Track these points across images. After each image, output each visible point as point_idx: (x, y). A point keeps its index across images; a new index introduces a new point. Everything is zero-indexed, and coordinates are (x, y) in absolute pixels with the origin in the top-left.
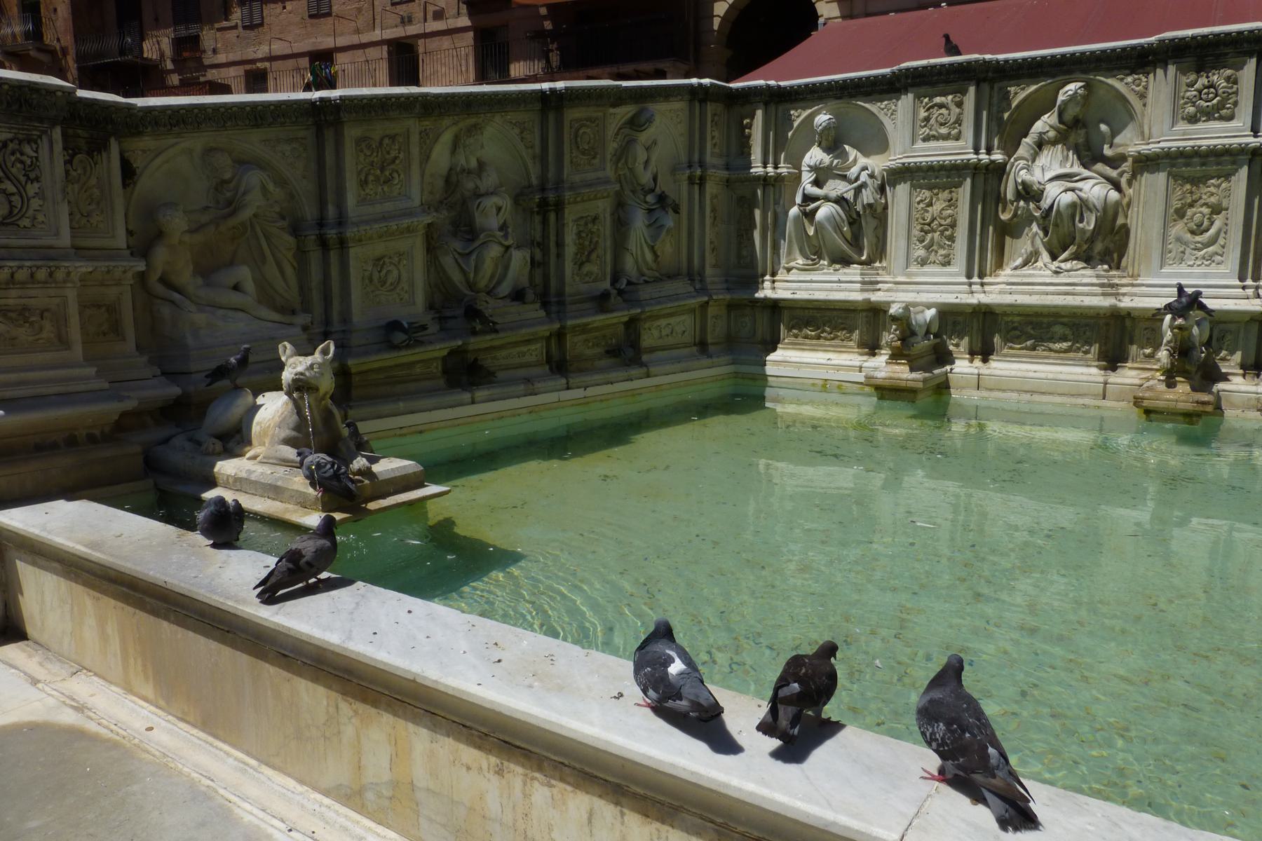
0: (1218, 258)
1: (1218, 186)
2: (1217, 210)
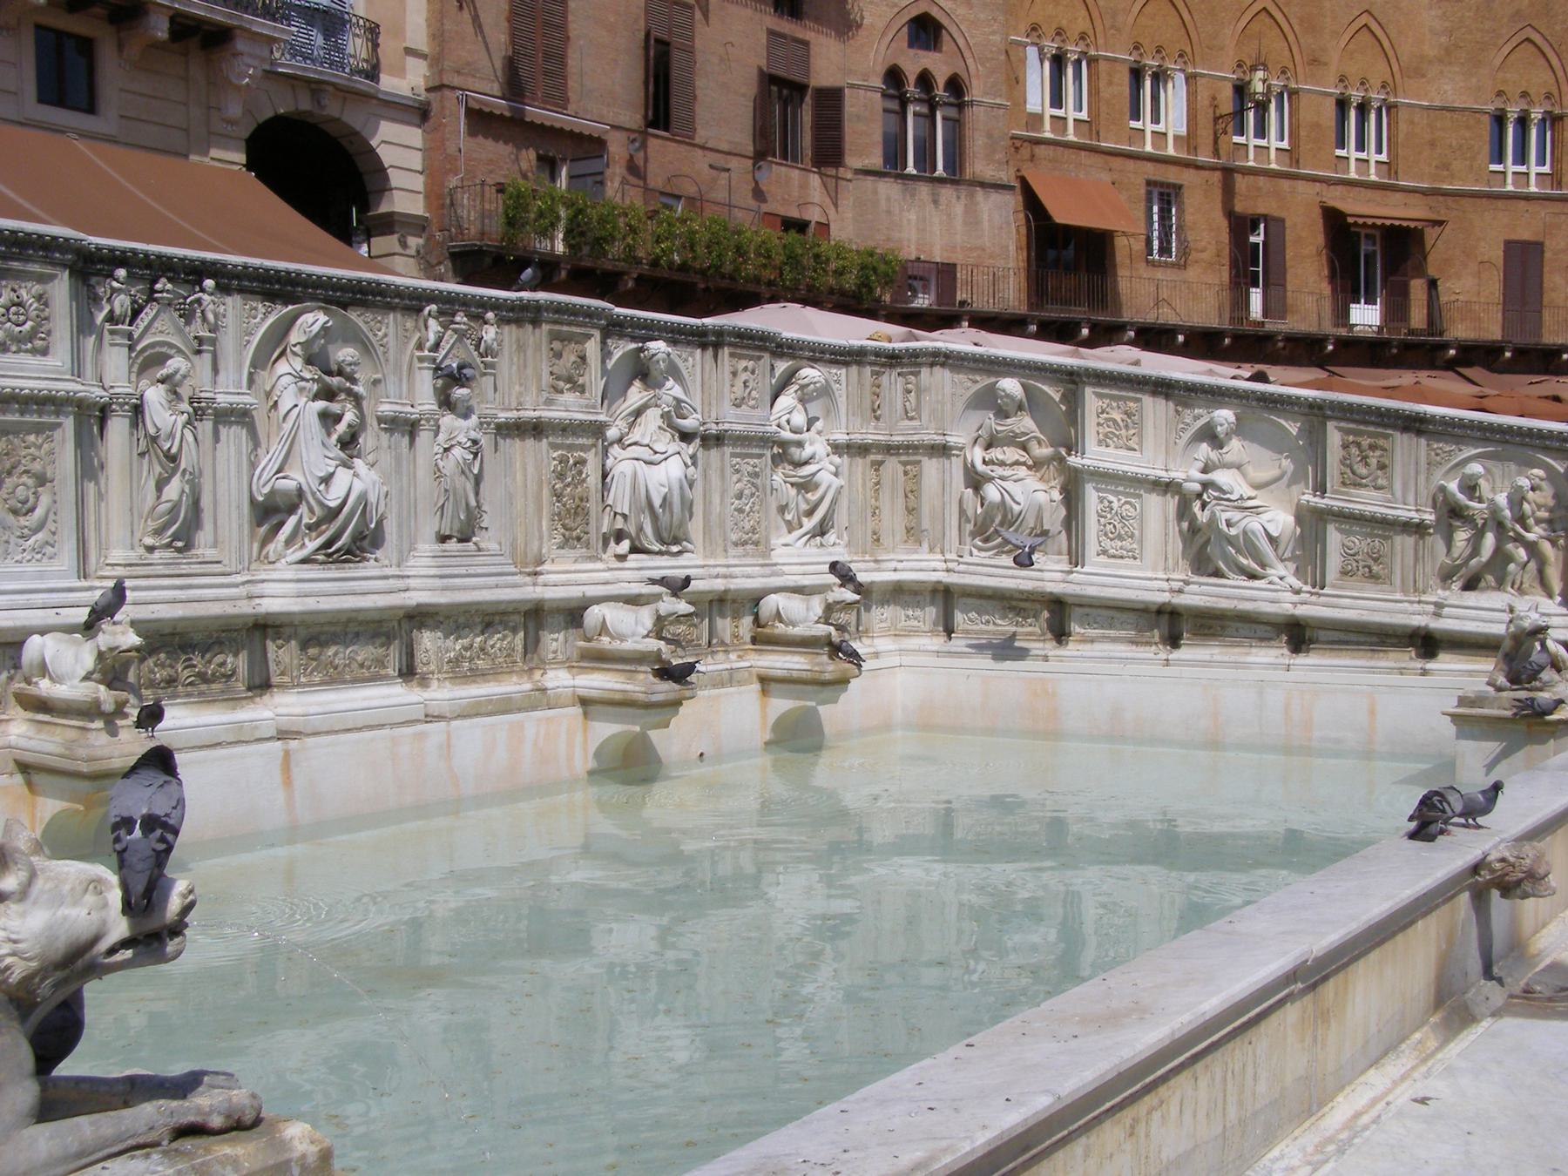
0: (49, 550)
1: (39, 447)
2: (42, 480)
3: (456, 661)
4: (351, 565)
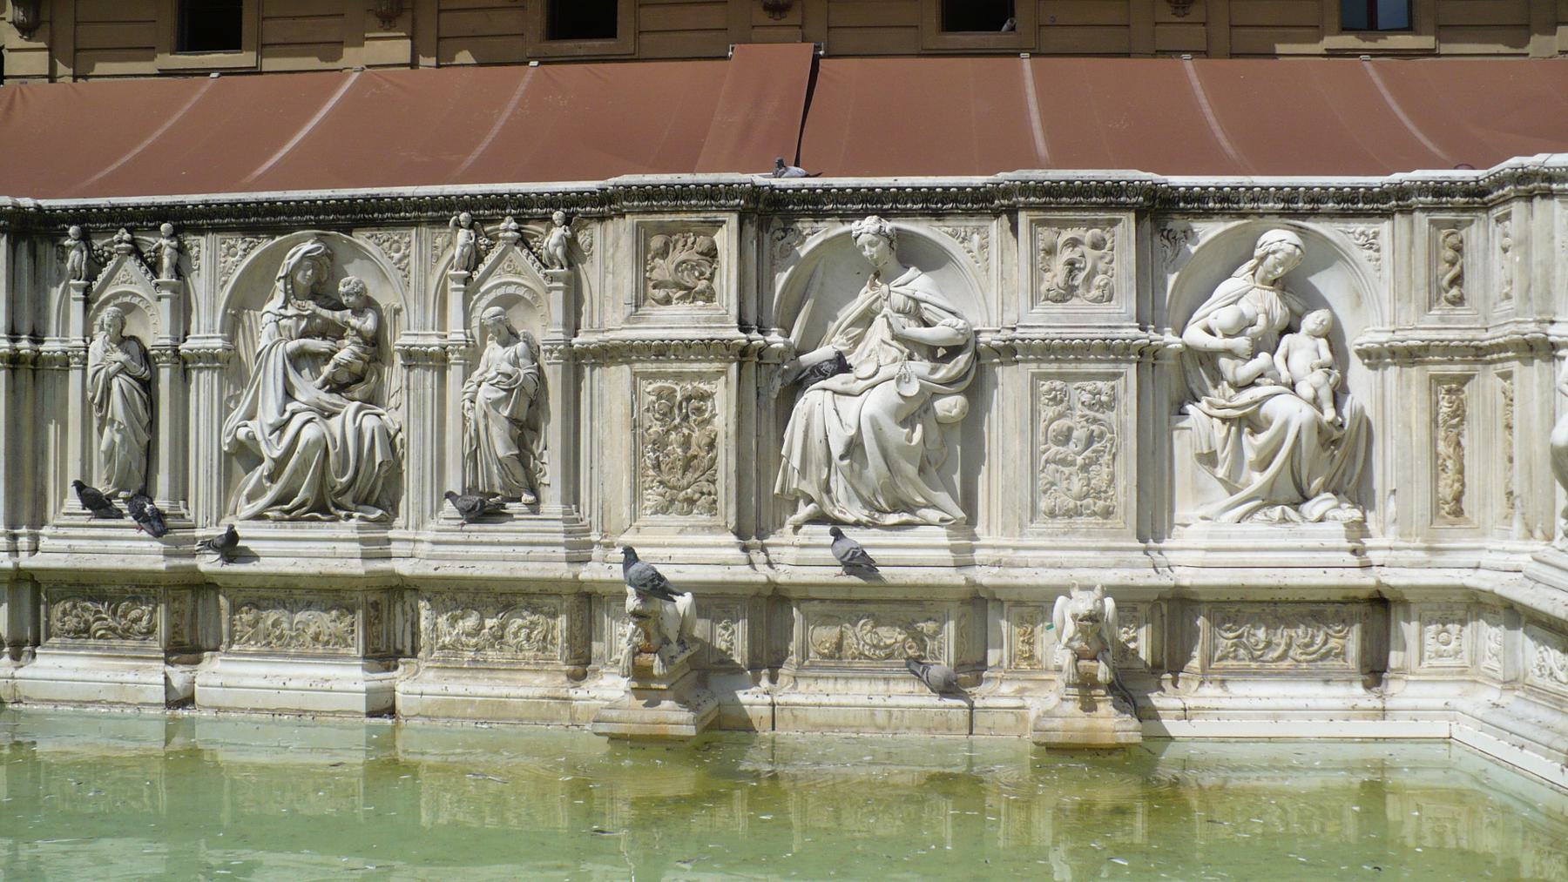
3: (456, 647)
4: (314, 524)
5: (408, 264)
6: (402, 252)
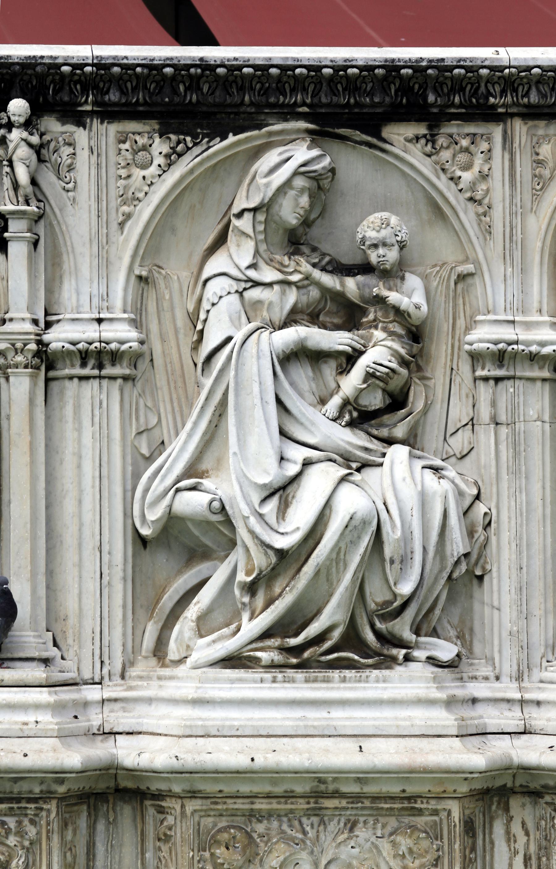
5: (488, 191)
6: (476, 169)
